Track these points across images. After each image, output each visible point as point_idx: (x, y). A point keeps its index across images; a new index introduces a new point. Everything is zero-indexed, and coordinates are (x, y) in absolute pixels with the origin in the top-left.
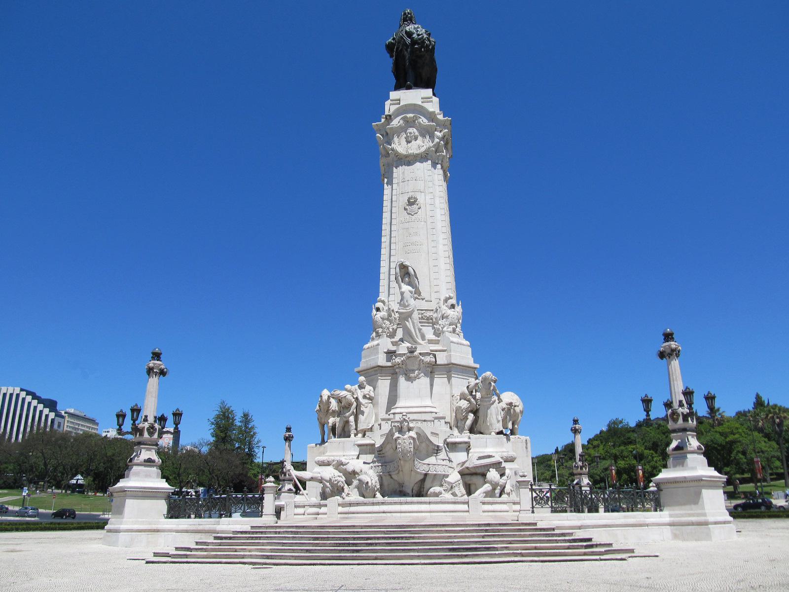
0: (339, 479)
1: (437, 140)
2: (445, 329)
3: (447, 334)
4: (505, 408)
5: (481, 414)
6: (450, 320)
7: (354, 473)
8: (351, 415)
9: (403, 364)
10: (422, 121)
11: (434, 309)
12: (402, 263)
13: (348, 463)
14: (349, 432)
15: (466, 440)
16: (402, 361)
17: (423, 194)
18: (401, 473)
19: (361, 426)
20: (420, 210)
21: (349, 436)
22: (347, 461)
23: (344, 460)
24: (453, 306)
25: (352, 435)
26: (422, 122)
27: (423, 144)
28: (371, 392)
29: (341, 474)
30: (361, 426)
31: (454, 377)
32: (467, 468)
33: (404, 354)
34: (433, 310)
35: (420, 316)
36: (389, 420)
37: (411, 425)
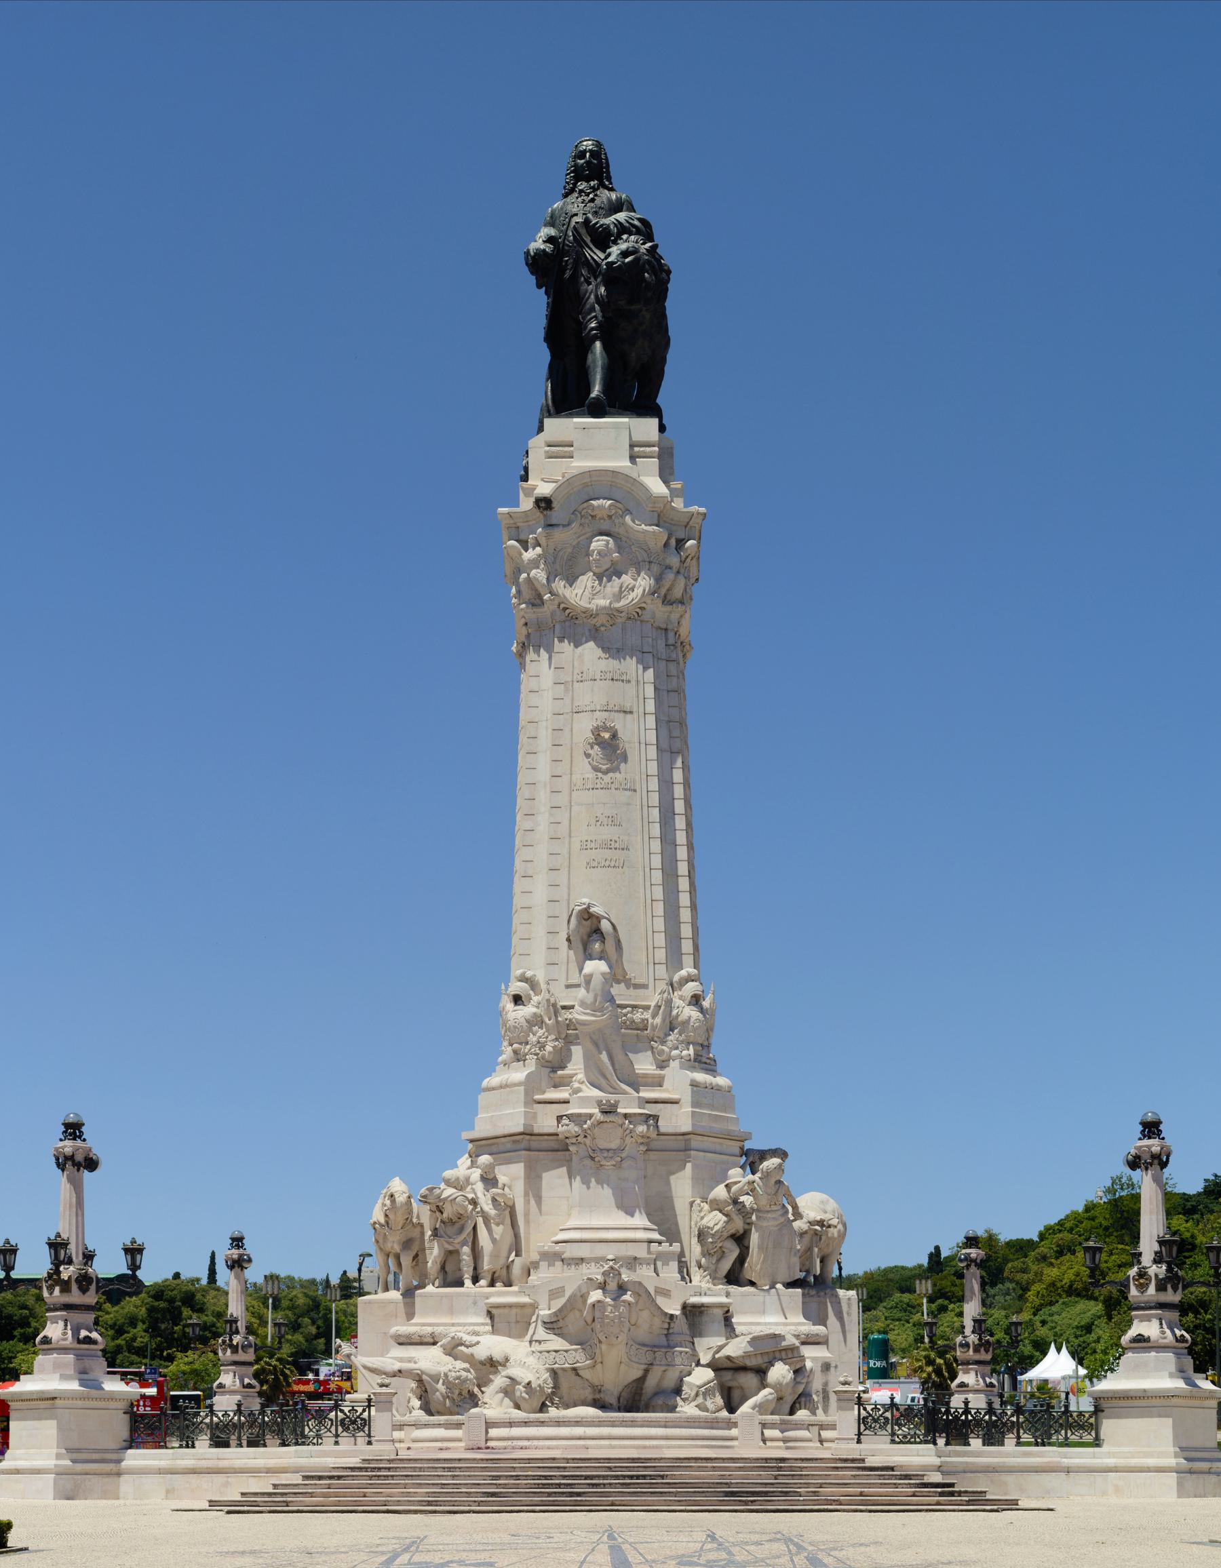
0: (464, 1374)
7: (492, 1365)
13: (478, 1343)
15: (724, 1300)
18: (599, 1366)
21: (460, 1284)
22: (475, 1339)
25: (468, 1283)
29: (466, 1365)
30: (486, 1265)
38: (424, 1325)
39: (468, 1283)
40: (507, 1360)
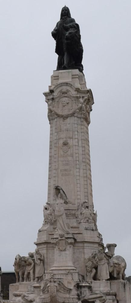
1: (81, 105)
2: (82, 221)
3: (83, 223)
4: (112, 266)
5: (99, 269)
6: (85, 216)
8: (31, 269)
9: (57, 243)
10: (71, 93)
11: (76, 209)
12: (57, 188)
14: (30, 278)
16: (57, 242)
17: (71, 139)
19: (37, 275)
20: (69, 149)
21: (30, 281)
23: (26, 295)
24: (87, 207)
25: (32, 281)
26: (71, 94)
27: (71, 108)
28: (42, 257)
30: (37, 275)
31: (86, 248)
32: (85, 299)
33: (57, 238)
34: (76, 210)
35: (69, 213)
36: (49, 273)
37: (55, 280)
38: (21, 291)
39: (32, 281)
40: (34, 301)
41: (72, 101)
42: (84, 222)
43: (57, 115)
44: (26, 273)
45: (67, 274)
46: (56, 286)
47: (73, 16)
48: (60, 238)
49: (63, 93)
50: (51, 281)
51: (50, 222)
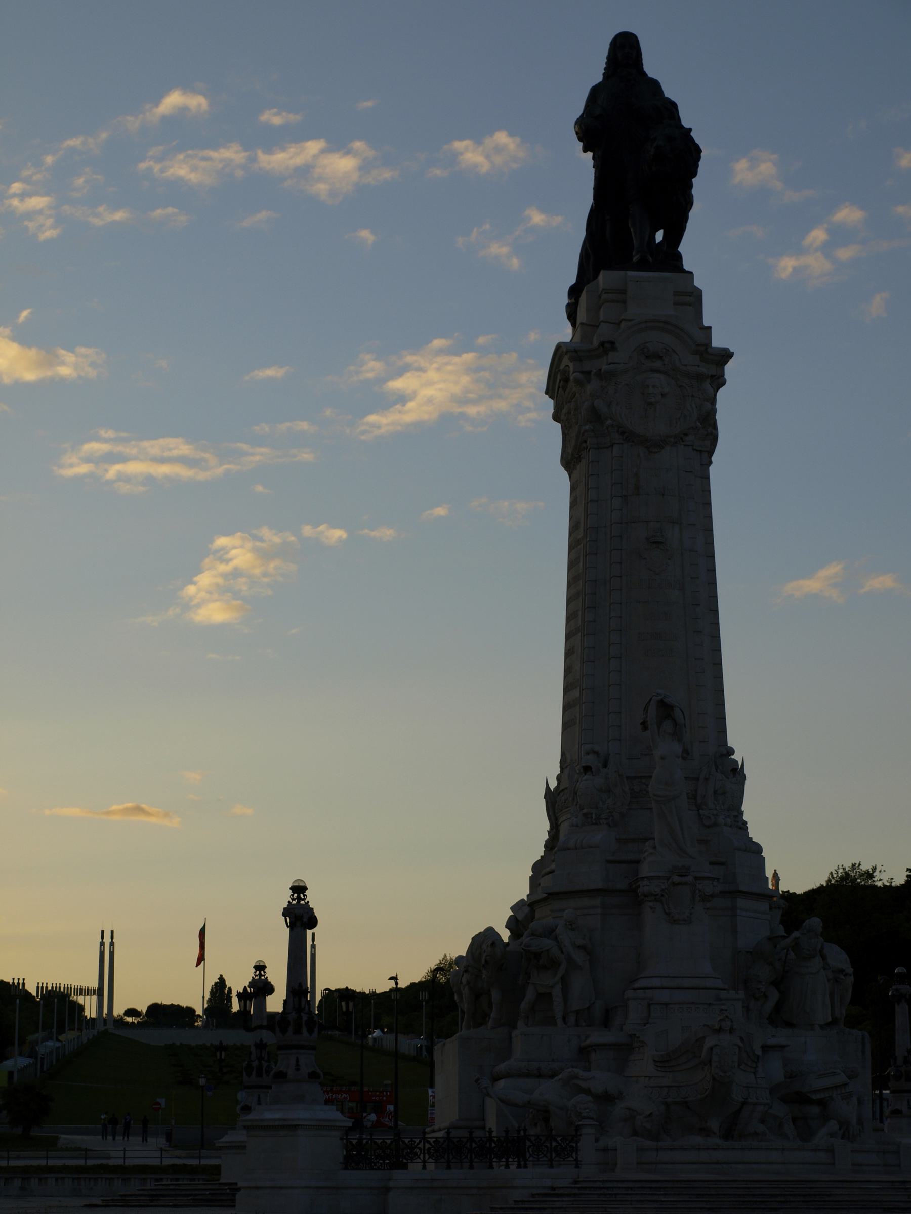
16: (663, 890)
41: (680, 387)
42: (725, 825)
43: (623, 433)
44: (530, 994)
45: (710, 1004)
46: (740, 1047)
47: (652, 67)
48: (676, 879)
49: (647, 357)
50: (720, 1030)
51: (606, 819)
